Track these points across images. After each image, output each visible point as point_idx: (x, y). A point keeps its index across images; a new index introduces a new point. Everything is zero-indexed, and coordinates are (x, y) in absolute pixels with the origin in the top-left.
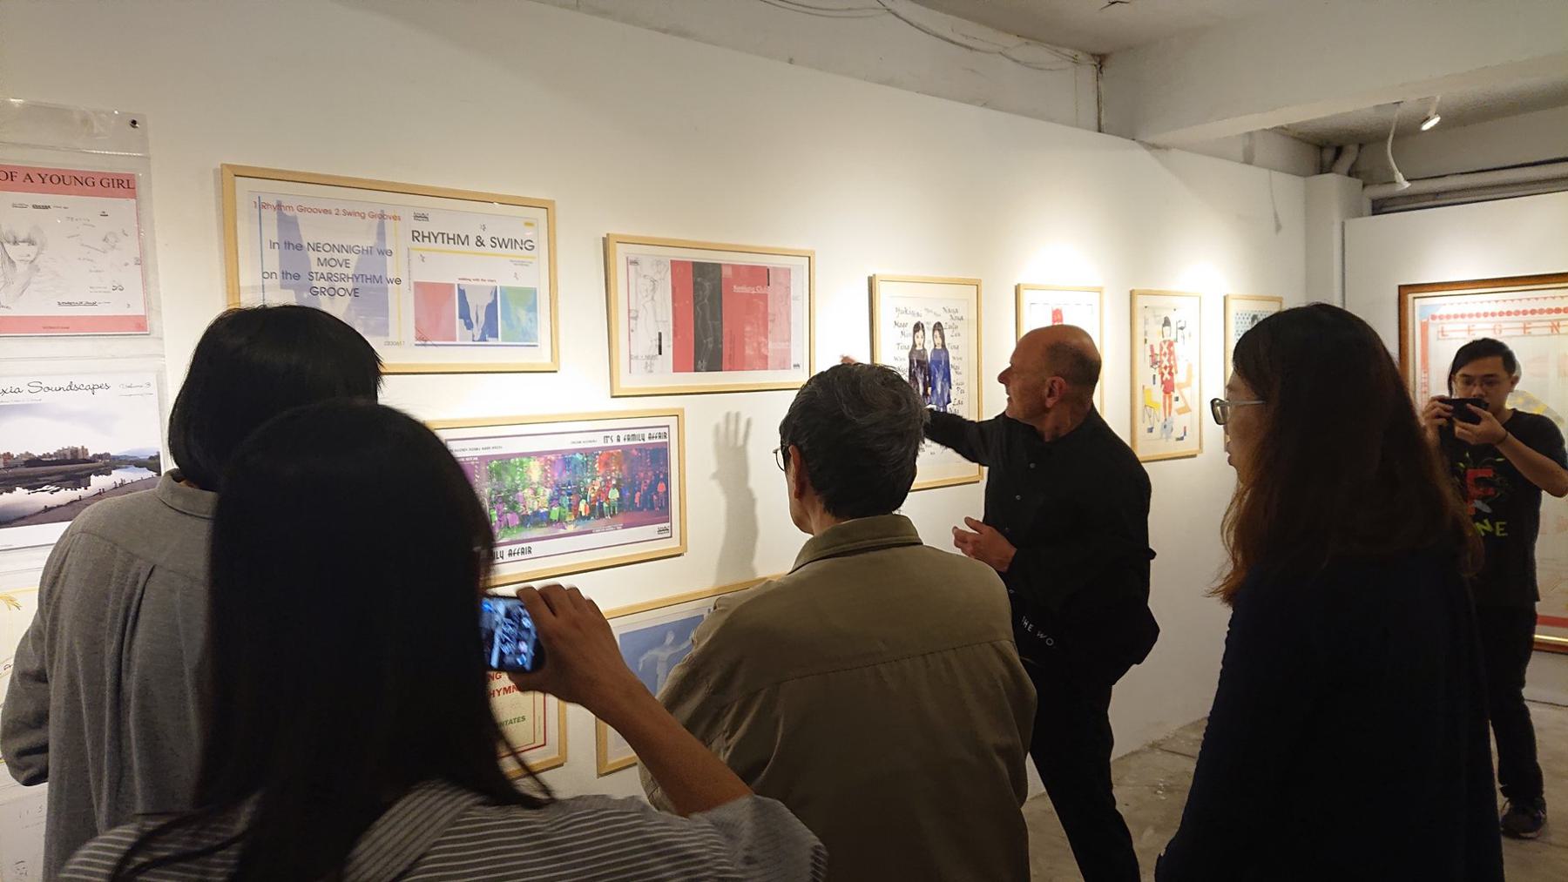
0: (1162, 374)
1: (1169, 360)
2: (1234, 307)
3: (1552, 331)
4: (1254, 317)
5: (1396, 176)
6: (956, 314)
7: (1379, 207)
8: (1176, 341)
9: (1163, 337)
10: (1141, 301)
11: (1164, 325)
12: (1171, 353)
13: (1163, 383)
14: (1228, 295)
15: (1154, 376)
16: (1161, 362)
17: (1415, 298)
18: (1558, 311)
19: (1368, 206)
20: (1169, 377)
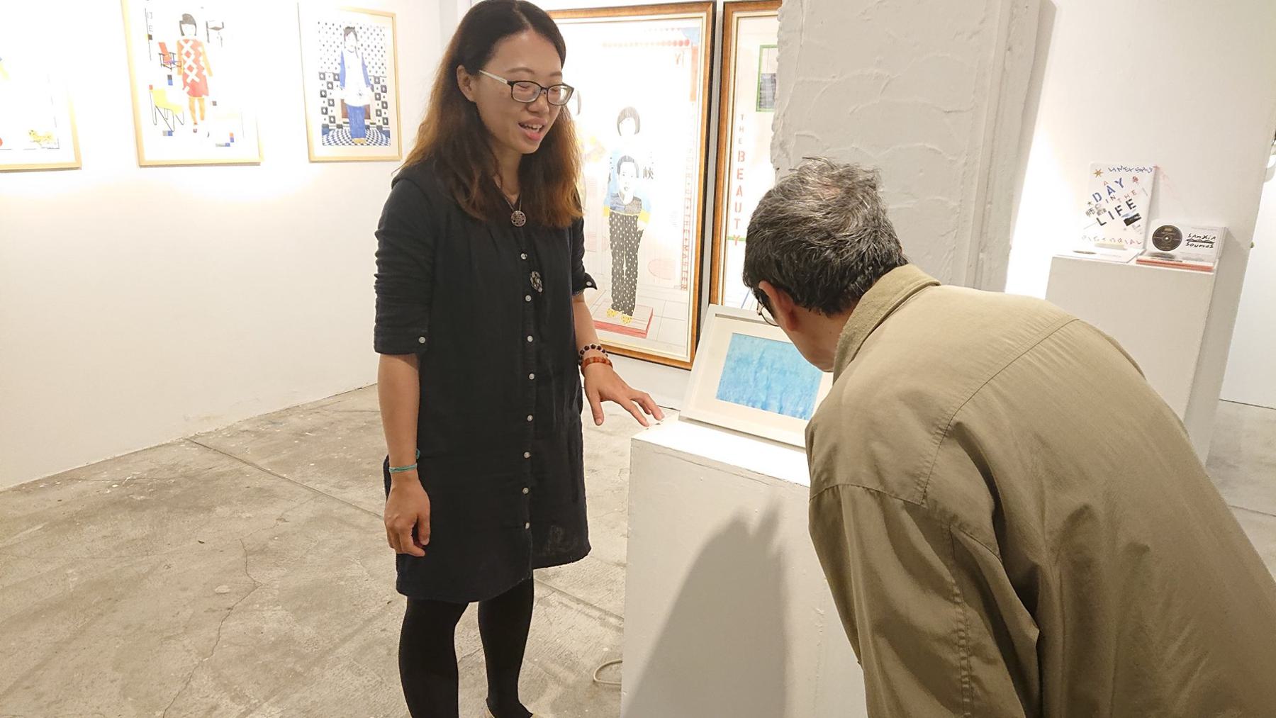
0: (185, 76)
1: (196, 61)
4: (349, 30)
9: (183, 34)
11: (181, 22)
12: (198, 54)
13: (185, 84)
15: (170, 77)
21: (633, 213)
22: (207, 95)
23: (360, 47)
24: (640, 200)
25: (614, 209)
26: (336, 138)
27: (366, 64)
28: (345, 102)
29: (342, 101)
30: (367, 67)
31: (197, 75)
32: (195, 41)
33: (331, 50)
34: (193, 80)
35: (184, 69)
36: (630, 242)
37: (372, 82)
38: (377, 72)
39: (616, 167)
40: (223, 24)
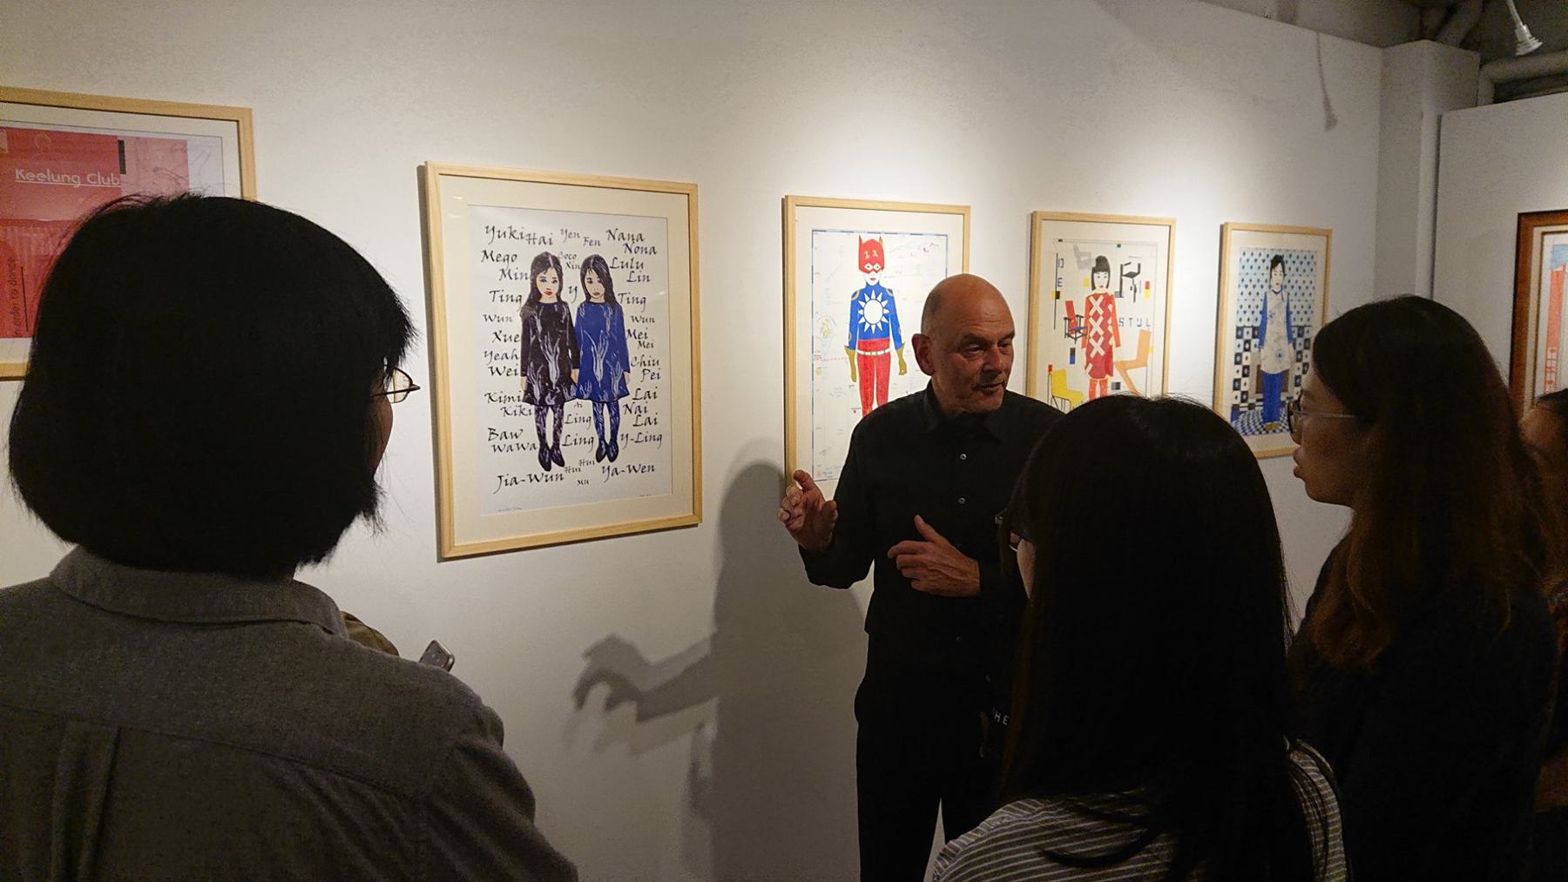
0: (1090, 348)
1: (1104, 326)
2: (1236, 242)
4: (1277, 260)
5: (1516, 31)
6: (640, 244)
7: (1506, 91)
8: (1121, 296)
9: (1094, 288)
10: (1048, 231)
11: (1094, 270)
12: (1107, 315)
14: (1227, 224)
15: (1073, 351)
16: (1088, 327)
17: (1544, 233)
19: (1486, 89)
20: (1102, 353)
22: (1112, 375)
26: (1246, 425)
27: (1291, 309)
28: (1262, 368)
29: (1259, 366)
30: (1292, 313)
31: (1102, 346)
32: (1105, 295)
33: (1254, 292)
34: (1098, 353)
35: (1090, 338)
37: (1295, 336)
38: (1302, 319)
40: (1139, 265)
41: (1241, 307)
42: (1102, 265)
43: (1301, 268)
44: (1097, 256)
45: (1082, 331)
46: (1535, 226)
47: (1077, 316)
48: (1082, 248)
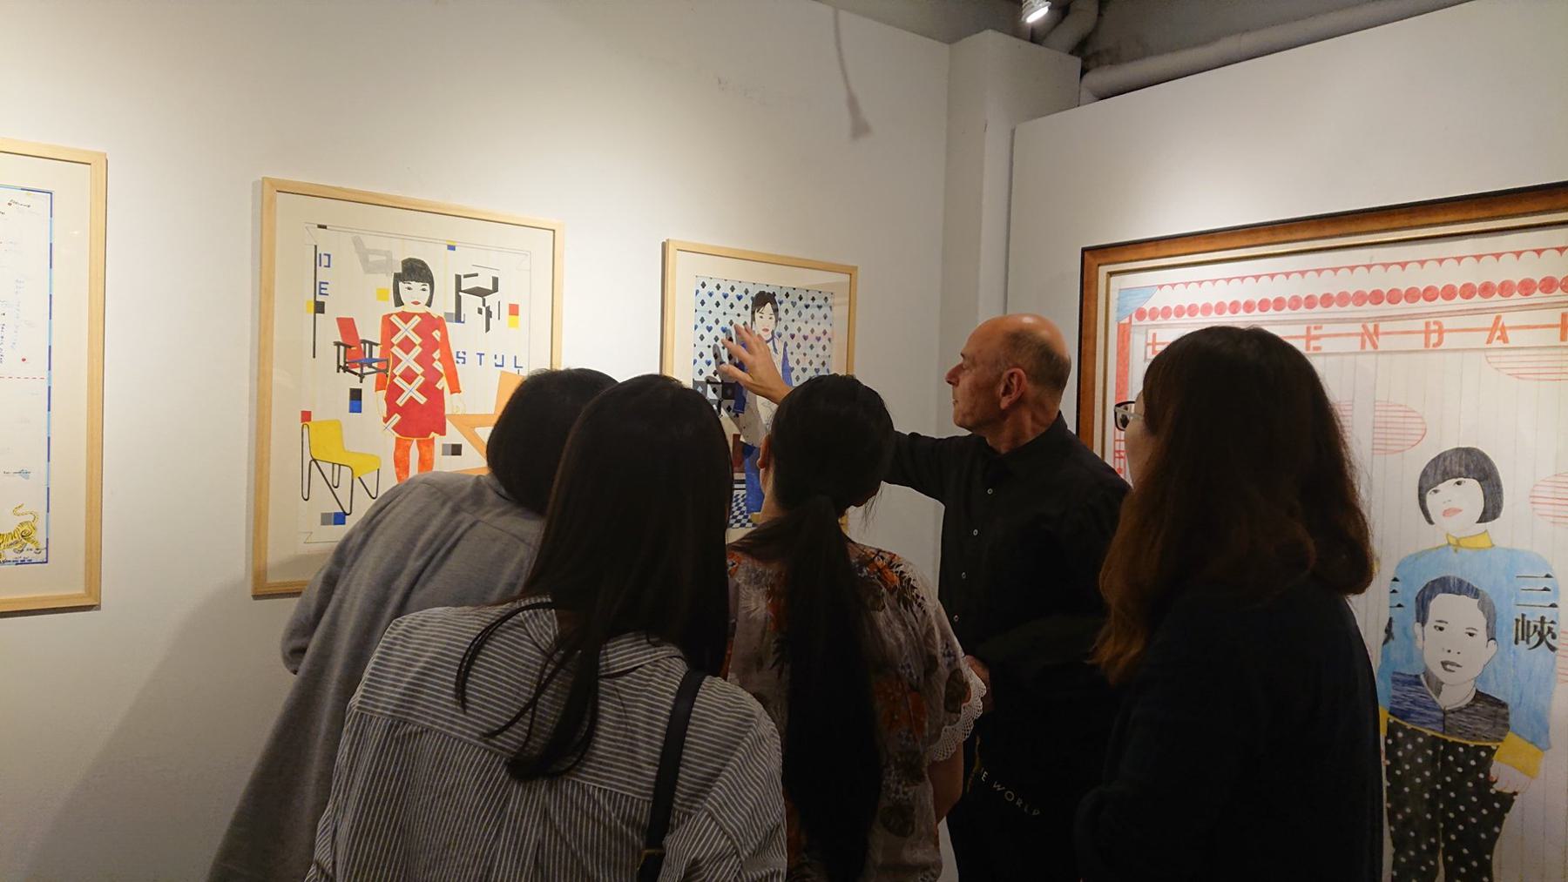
0: (395, 392)
1: (424, 360)
3: (1363, 346)
4: (762, 299)
9: (399, 302)
13: (392, 408)
14: (668, 240)
15: (356, 395)
16: (388, 361)
17: (1111, 274)
18: (1377, 297)
20: (422, 400)
21: (1474, 736)
22: (442, 432)
23: (783, 331)
24: (1504, 705)
25: (1402, 718)
27: (792, 364)
30: (792, 369)
32: (426, 317)
34: (412, 400)
36: (1462, 818)
39: (1411, 606)
40: (495, 280)
41: (701, 355)
42: (415, 271)
43: (807, 313)
44: (406, 257)
45: (375, 365)
46: (1099, 265)
47: (364, 342)
48: (370, 242)
